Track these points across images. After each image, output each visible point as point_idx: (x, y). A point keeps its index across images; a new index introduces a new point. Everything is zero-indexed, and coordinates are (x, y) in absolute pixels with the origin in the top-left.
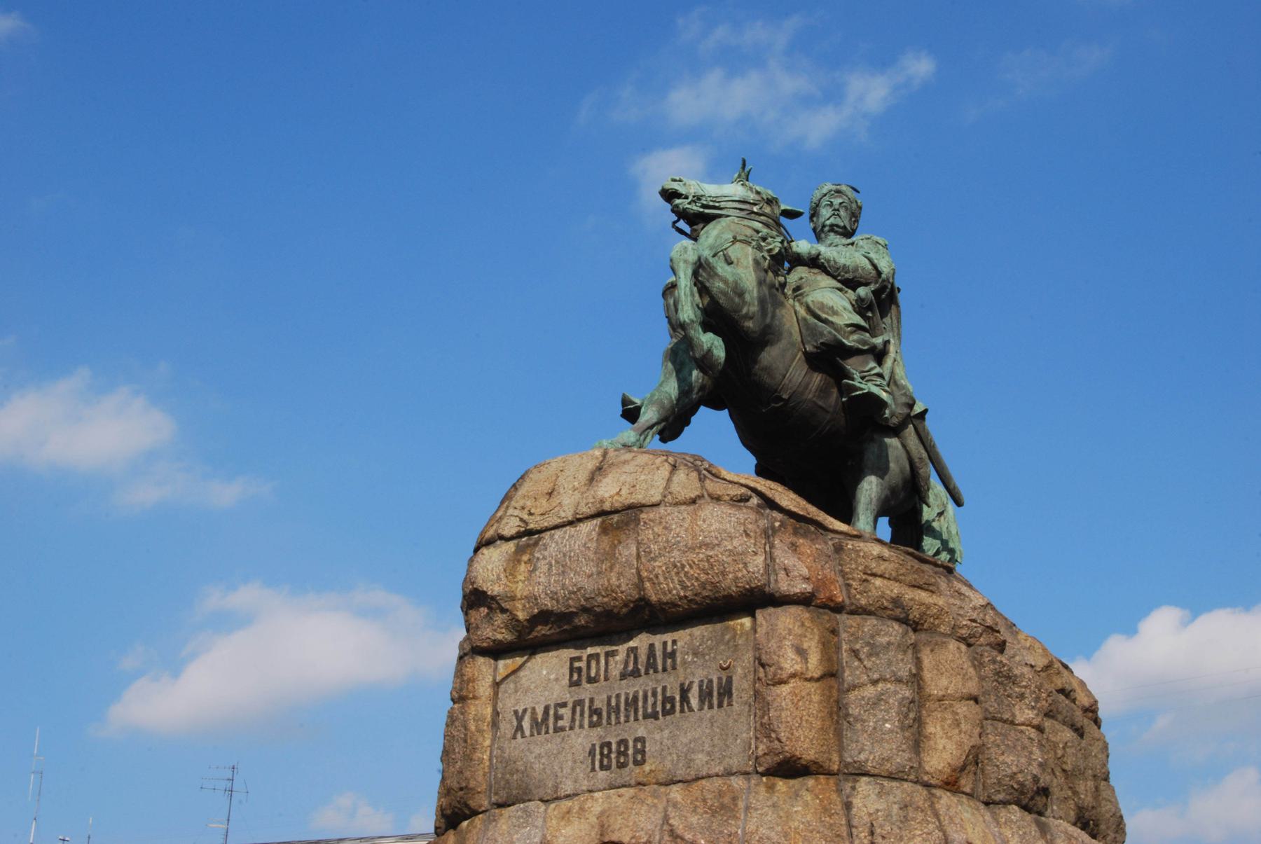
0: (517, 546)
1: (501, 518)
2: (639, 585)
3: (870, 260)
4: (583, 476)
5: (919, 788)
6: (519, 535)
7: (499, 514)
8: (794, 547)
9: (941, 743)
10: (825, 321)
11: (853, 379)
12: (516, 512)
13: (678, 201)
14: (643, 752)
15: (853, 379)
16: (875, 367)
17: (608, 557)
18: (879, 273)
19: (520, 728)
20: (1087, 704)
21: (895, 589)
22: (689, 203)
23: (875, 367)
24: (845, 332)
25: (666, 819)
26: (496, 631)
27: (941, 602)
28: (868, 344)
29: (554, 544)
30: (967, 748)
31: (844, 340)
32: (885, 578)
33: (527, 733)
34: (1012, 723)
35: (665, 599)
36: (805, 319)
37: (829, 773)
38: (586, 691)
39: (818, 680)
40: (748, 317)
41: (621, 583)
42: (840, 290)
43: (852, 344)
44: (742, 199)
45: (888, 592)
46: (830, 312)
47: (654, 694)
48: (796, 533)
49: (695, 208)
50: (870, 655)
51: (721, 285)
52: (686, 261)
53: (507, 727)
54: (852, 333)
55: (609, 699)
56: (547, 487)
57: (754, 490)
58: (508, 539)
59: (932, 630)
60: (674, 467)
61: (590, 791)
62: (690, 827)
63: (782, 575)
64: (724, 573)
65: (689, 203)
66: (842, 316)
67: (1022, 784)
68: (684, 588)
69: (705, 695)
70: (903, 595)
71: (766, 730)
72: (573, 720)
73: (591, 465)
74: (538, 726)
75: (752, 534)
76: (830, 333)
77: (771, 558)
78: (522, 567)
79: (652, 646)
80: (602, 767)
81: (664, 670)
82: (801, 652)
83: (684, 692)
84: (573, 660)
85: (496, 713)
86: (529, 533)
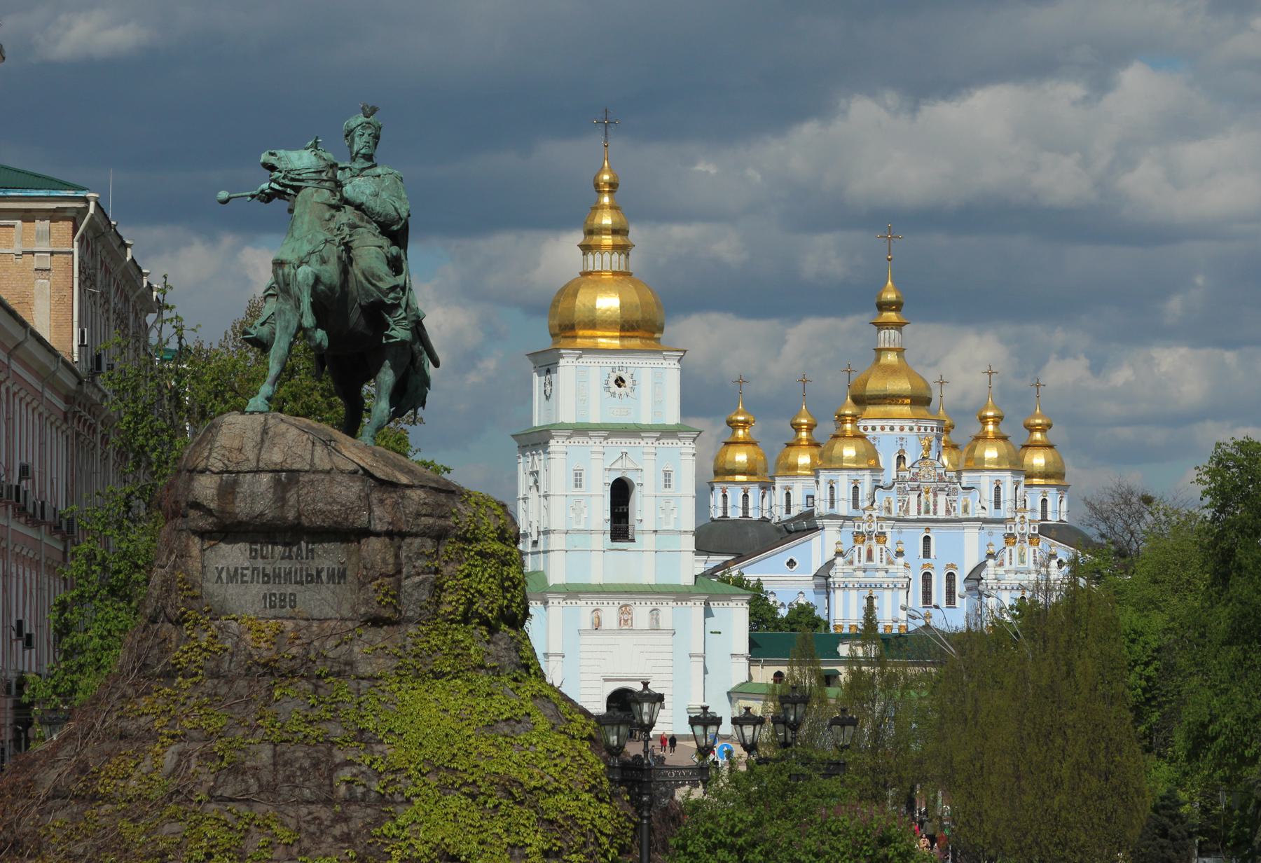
0: (222, 480)
1: (208, 458)
2: (299, 515)
3: (396, 210)
4: (259, 439)
6: (222, 472)
8: (381, 501)
11: (387, 326)
13: (276, 174)
14: (295, 602)
17: (281, 500)
19: (220, 577)
21: (431, 521)
22: (283, 178)
27: (451, 522)
33: (225, 581)
36: (361, 282)
38: (260, 563)
39: (392, 576)
41: (291, 515)
42: (380, 247)
48: (380, 491)
49: (287, 182)
52: (308, 285)
53: (213, 575)
55: (274, 569)
56: (236, 444)
57: (363, 468)
58: (213, 473)
68: (324, 521)
69: (331, 577)
72: (253, 578)
73: (259, 429)
80: (271, 607)
81: (307, 558)
83: (319, 572)
85: (203, 567)
86: (231, 472)
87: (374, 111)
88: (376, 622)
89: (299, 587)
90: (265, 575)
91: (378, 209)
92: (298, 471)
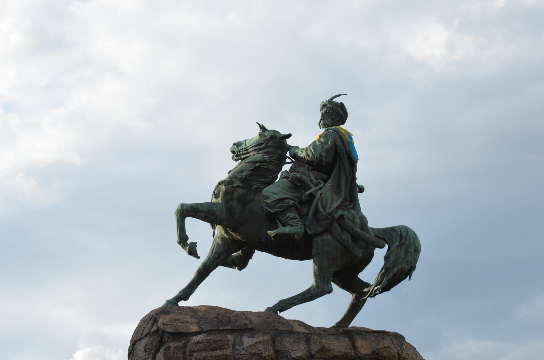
16: (290, 216)
22: (236, 156)
23: (290, 216)
24: (272, 206)
28: (284, 207)
31: (270, 211)
32: (199, 351)
43: (275, 210)
44: (257, 144)
45: (199, 357)
46: (266, 198)
51: (203, 214)
54: (276, 204)
65: (235, 157)
66: (271, 198)
70: (207, 355)
75: (148, 350)
76: (266, 209)
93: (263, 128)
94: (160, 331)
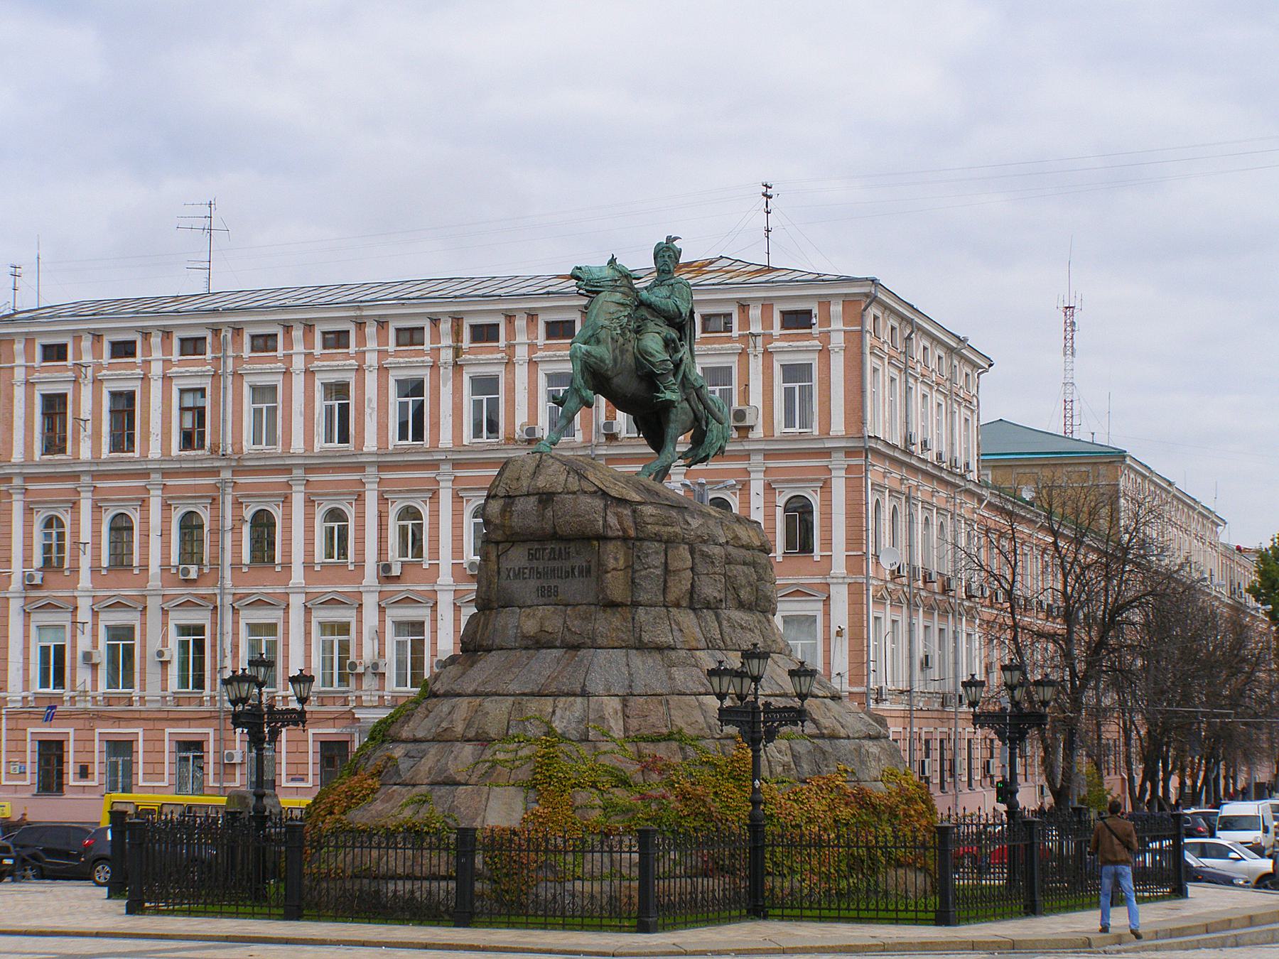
1: (498, 486)
4: (531, 470)
5: (663, 609)
7: (497, 483)
8: (616, 514)
9: (673, 589)
10: (647, 360)
11: (658, 390)
12: (504, 486)
13: (580, 283)
14: (557, 592)
15: (658, 390)
18: (681, 314)
19: (509, 575)
20: (759, 544)
25: (565, 622)
26: (498, 536)
27: (678, 529)
29: (520, 505)
30: (684, 591)
34: (708, 574)
35: (565, 534)
36: (638, 359)
37: (627, 605)
38: (535, 564)
40: (607, 370)
41: (548, 527)
47: (562, 567)
49: (587, 288)
50: (644, 557)
53: (503, 575)
56: (516, 475)
59: (673, 542)
60: (569, 473)
61: (537, 605)
62: (573, 626)
63: (609, 530)
64: (586, 528)
67: (708, 601)
69: (581, 572)
71: (603, 590)
74: (516, 576)
77: (605, 520)
78: (508, 514)
79: (560, 549)
82: (616, 559)
83: (573, 569)
84: (529, 549)
85: (499, 568)
86: (509, 497)
87: (676, 239)
88: (612, 605)
89: (560, 580)
90: (538, 573)
91: (663, 307)
92: (554, 494)
93: (612, 261)
94: (600, 493)
